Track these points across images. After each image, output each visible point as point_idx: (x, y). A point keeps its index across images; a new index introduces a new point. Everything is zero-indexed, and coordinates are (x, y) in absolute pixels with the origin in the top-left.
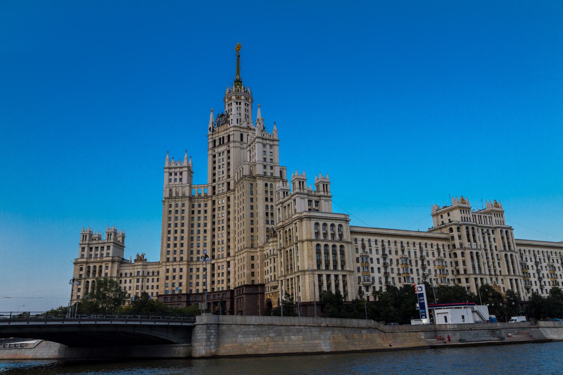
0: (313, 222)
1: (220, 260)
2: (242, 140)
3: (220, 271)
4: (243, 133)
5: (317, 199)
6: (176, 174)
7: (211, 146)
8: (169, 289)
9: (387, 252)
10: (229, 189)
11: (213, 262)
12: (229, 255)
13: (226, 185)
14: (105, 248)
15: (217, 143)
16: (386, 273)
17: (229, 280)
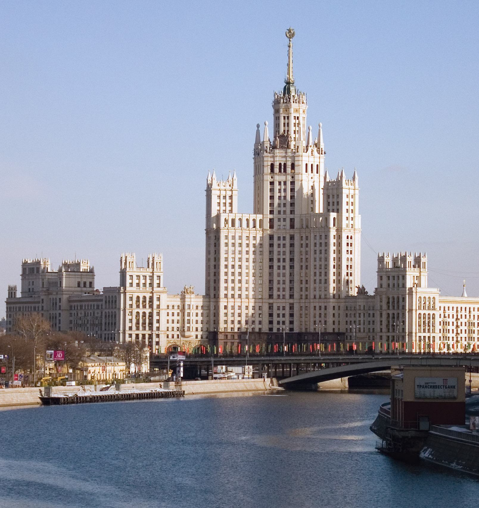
0: (418, 296)
1: (280, 301)
2: (306, 172)
3: (281, 312)
4: (307, 163)
5: (418, 274)
6: (225, 197)
7: (267, 170)
8: (230, 326)
9: (459, 317)
10: (292, 226)
11: (271, 301)
12: (291, 296)
13: (288, 221)
14: (155, 277)
15: (277, 170)
16: (457, 333)
17: (291, 322)
